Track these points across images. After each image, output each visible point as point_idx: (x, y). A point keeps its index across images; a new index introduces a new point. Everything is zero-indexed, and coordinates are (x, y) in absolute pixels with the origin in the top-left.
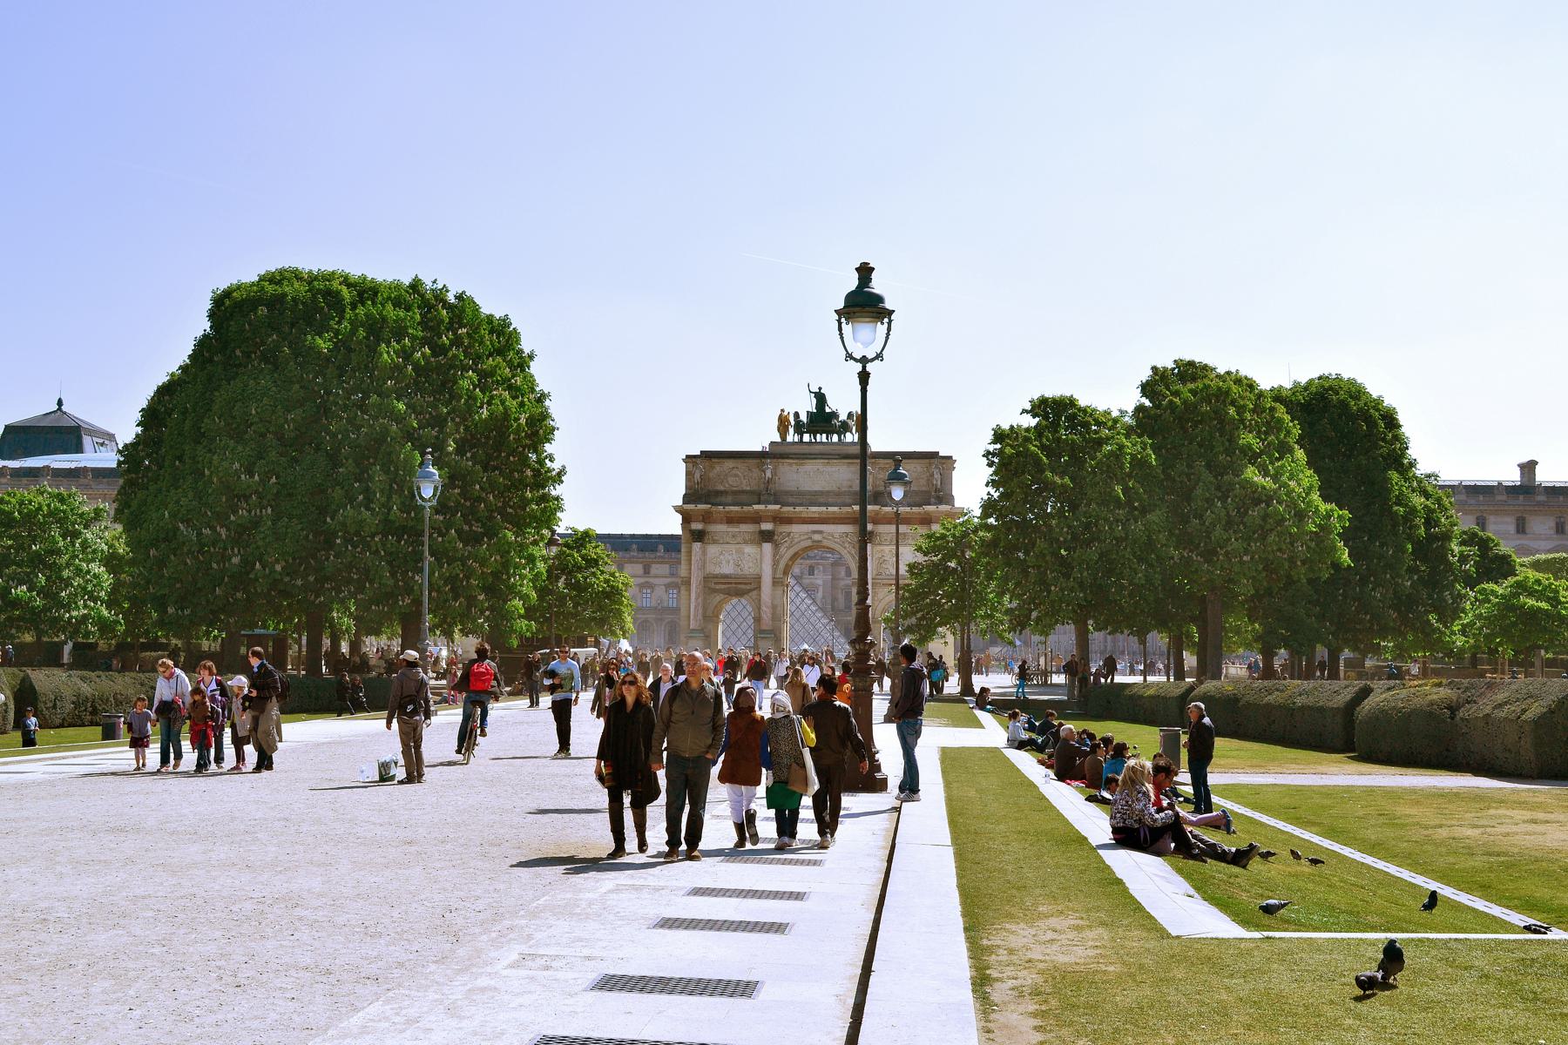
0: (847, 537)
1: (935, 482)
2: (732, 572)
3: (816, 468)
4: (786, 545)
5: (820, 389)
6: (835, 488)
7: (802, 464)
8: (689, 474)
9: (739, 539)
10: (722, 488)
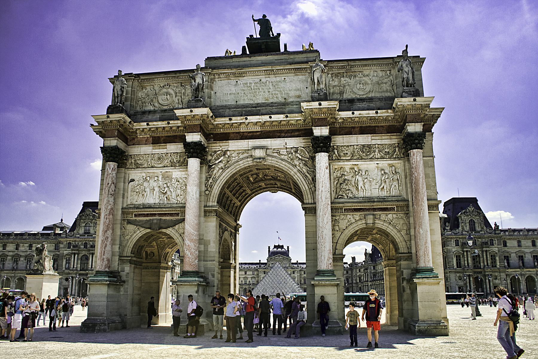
1: (405, 76)
2: (157, 201)
4: (221, 165)
5: (264, 16)
6: (283, 100)
7: (241, 75)
9: (166, 162)
10: (152, 108)
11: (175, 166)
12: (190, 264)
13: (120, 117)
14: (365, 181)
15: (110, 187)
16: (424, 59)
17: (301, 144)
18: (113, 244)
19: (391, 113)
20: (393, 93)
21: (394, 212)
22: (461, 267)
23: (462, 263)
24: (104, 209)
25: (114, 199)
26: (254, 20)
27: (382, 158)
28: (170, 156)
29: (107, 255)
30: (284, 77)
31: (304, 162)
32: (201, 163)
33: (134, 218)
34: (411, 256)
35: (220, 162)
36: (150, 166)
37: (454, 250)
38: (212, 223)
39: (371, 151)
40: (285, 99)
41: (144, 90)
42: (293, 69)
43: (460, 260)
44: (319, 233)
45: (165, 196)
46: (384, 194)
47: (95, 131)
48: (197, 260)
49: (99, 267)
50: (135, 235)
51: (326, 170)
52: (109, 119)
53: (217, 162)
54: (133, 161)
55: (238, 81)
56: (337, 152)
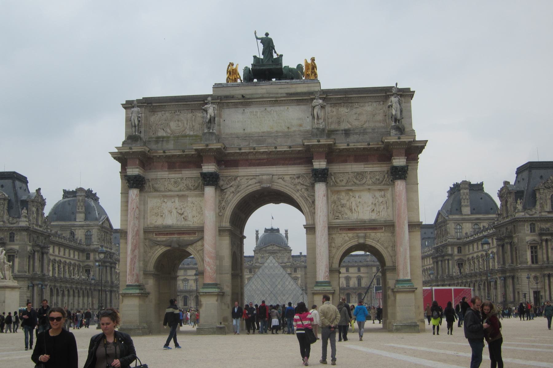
0: (298, 178)
1: (394, 113)
3: (262, 109)
4: (232, 189)
5: (267, 34)
6: (286, 130)
8: (128, 120)
9: (182, 186)
11: (191, 189)
12: (211, 277)
13: (142, 149)
14: (358, 204)
15: (135, 212)
16: (414, 92)
17: (303, 171)
18: (139, 261)
19: (381, 145)
20: (386, 124)
21: (382, 231)
22: (537, 263)
23: (540, 257)
24: (131, 231)
25: (139, 222)
26: (257, 38)
27: (374, 183)
28: (186, 180)
29: (136, 271)
30: (287, 107)
31: (305, 187)
32: (216, 189)
33: (155, 237)
34: (396, 269)
35: (231, 186)
36: (167, 190)
37: (528, 238)
38: (226, 242)
39: (364, 178)
40: (288, 128)
41: (156, 115)
42: (296, 100)
43: (536, 252)
44: (318, 251)
45: (182, 217)
46: (374, 216)
47: (113, 157)
48: (215, 274)
49: (129, 281)
50: (157, 252)
51: (323, 197)
52: (131, 150)
53: (228, 186)
54: (151, 184)
55: (245, 109)
56: (334, 178)
